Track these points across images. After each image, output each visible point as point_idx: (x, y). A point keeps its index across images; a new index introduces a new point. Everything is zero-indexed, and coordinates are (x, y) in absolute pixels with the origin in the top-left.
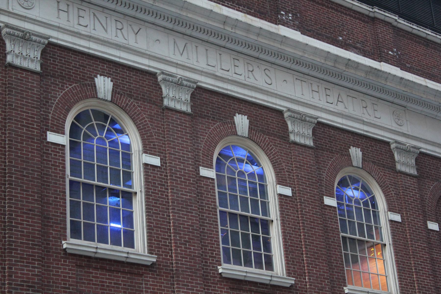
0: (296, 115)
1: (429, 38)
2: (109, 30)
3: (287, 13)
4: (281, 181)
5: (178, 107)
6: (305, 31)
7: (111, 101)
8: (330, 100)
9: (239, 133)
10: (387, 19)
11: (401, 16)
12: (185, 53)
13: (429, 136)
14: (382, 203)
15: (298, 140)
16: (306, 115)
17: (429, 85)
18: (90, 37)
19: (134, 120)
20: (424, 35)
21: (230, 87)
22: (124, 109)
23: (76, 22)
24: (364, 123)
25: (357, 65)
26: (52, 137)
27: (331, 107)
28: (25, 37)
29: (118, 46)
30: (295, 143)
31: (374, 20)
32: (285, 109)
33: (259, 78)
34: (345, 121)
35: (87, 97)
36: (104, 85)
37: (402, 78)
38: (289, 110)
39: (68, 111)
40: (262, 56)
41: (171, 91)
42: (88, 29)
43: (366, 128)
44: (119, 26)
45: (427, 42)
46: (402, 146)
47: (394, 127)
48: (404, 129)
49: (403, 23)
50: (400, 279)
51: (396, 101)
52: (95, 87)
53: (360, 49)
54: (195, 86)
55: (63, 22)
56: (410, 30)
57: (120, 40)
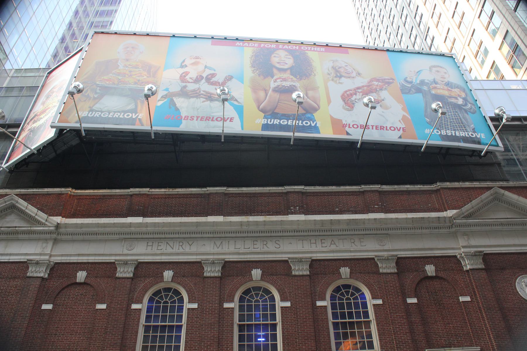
0: (295, 260)
1: (409, 189)
2: (174, 248)
3: (295, 207)
4: (283, 299)
5: (212, 275)
6: (306, 213)
7: (172, 281)
8: (324, 245)
9: (254, 279)
10: (373, 189)
11: (382, 184)
12: (221, 247)
13: (421, 246)
14: (368, 295)
15: (297, 273)
16: (301, 258)
17: (415, 216)
18: (162, 254)
19: (184, 287)
20: (406, 189)
21: (249, 256)
22: (179, 283)
23: (156, 249)
24: (351, 251)
25: (339, 221)
26: (134, 306)
27: (324, 249)
28: (126, 263)
29: (178, 254)
30: (295, 276)
31: (363, 192)
32: (287, 259)
33: (271, 246)
34: (335, 254)
35: (157, 283)
36: (168, 274)
37: (375, 219)
38: (289, 258)
39: (146, 292)
40: (273, 234)
41: (209, 268)
42: (162, 251)
43: (353, 254)
44: (181, 244)
45: (408, 192)
46: (381, 258)
47: (381, 248)
48: (386, 247)
49: (386, 188)
50: (380, 340)
51: (378, 232)
52: (163, 276)
53: (352, 211)
54: (223, 262)
55: (149, 251)
56: (393, 189)
57: (181, 250)
